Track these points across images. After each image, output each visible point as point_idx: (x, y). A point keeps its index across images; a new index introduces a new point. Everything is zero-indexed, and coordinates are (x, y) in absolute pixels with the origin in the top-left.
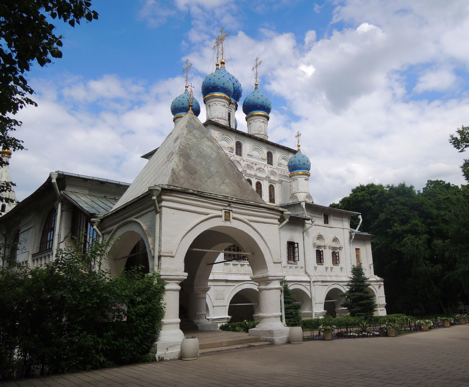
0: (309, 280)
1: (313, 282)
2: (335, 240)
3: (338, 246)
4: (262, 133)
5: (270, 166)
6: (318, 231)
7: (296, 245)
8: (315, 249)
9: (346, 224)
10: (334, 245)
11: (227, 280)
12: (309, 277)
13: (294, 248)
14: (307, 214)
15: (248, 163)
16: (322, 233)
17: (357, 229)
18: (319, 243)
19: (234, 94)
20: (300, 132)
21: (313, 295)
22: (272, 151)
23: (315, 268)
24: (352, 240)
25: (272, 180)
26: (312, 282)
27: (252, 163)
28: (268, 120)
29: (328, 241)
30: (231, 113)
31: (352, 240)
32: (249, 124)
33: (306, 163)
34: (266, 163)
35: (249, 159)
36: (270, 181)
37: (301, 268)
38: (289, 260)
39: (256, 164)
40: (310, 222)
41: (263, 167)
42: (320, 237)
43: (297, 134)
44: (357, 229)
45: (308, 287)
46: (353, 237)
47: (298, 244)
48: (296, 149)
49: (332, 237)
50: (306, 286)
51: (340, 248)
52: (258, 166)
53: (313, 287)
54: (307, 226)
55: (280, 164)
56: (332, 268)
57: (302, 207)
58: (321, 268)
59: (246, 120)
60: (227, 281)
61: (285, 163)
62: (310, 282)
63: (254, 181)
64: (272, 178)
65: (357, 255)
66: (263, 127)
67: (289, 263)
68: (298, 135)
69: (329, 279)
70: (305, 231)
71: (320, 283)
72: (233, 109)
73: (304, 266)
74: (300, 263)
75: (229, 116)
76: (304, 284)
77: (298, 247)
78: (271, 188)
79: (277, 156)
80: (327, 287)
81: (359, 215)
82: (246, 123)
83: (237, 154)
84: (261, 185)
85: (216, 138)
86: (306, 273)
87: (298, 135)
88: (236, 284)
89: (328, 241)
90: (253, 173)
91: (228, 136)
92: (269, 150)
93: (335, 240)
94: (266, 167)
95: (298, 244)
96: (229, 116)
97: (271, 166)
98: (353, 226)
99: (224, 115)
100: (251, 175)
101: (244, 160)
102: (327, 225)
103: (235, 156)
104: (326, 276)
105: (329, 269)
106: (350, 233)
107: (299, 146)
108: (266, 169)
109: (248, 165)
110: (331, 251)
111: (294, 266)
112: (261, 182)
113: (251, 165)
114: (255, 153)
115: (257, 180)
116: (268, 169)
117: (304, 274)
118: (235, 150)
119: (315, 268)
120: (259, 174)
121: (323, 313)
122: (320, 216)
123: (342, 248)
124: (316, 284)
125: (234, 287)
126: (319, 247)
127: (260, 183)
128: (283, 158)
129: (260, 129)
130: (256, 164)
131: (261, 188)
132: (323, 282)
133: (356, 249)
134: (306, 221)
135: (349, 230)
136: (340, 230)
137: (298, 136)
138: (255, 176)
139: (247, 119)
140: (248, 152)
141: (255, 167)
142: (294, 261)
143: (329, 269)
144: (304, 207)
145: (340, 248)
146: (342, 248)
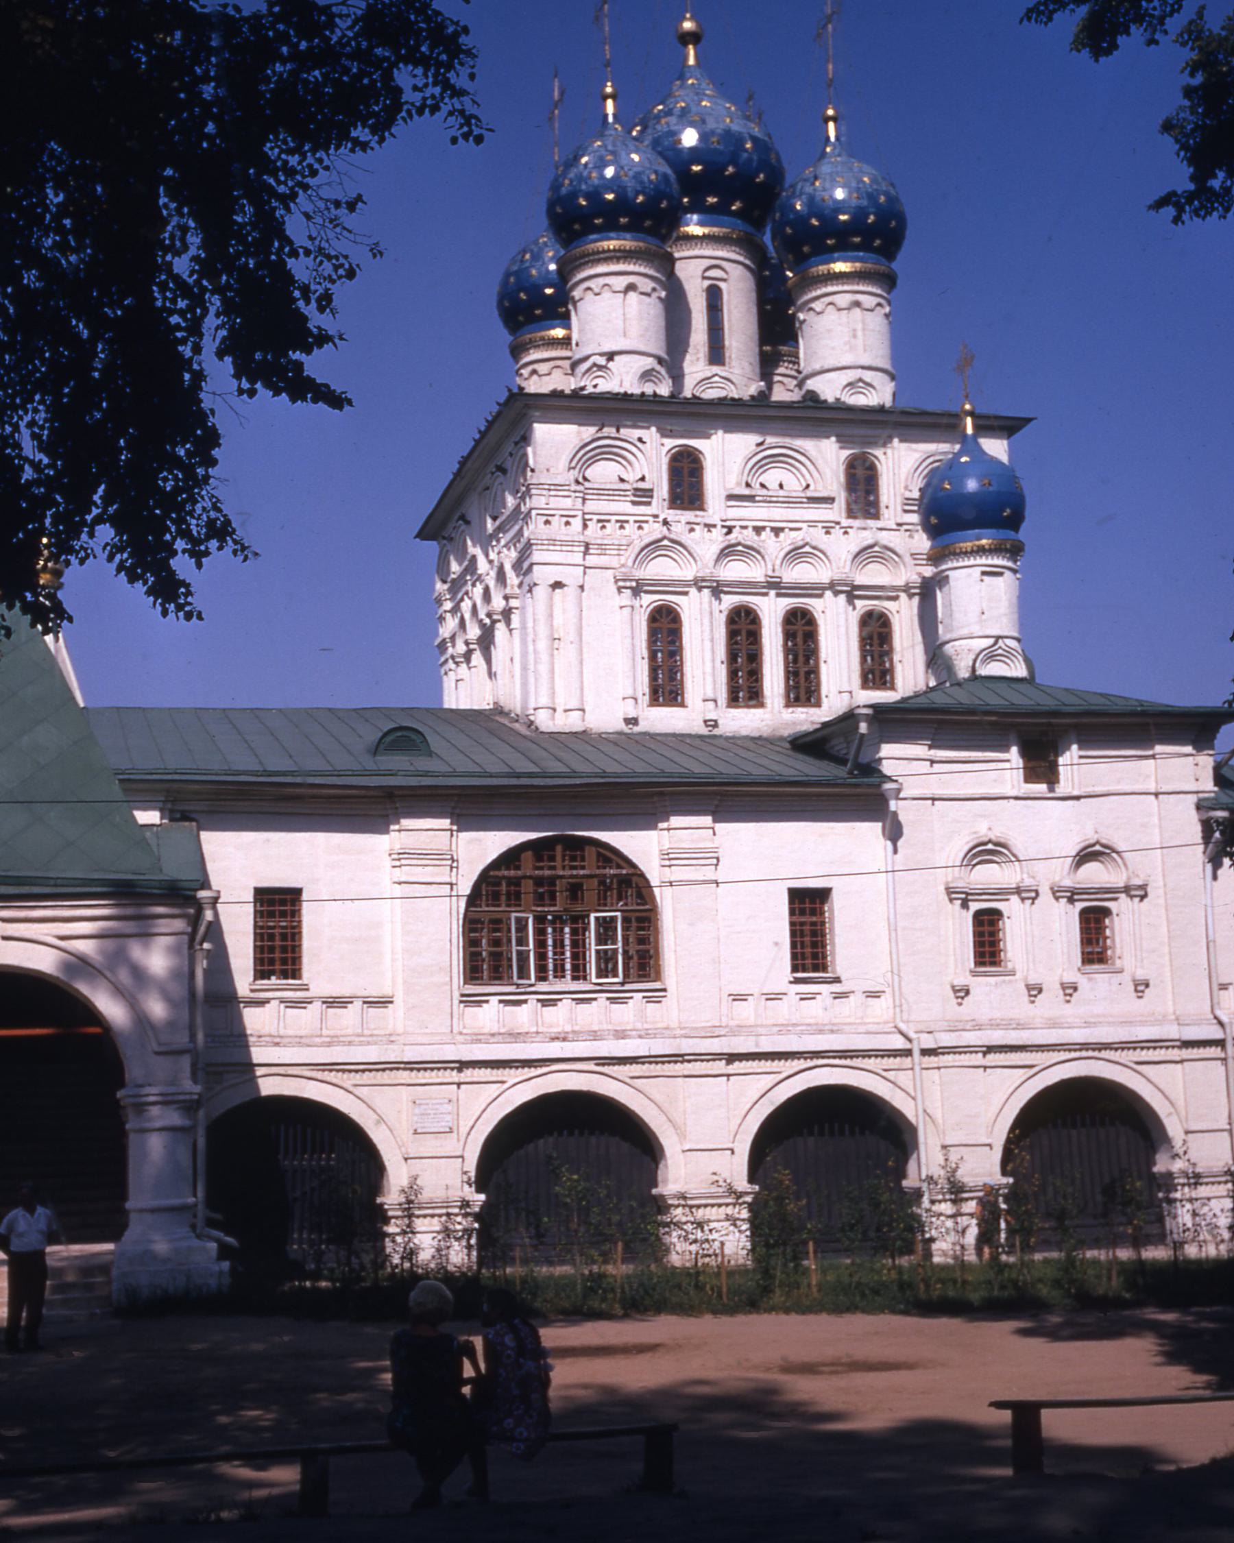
27: (758, 530)
30: (722, 285)
34: (836, 512)
38: (795, 969)
39: (777, 531)
41: (817, 536)
51: (1139, 892)
52: (789, 539)
56: (1070, 989)
62: (908, 1053)
71: (978, 1059)
88: (512, 1075)
94: (837, 532)
105: (1052, 993)
115: (786, 603)
125: (494, 1089)
138: (775, 585)
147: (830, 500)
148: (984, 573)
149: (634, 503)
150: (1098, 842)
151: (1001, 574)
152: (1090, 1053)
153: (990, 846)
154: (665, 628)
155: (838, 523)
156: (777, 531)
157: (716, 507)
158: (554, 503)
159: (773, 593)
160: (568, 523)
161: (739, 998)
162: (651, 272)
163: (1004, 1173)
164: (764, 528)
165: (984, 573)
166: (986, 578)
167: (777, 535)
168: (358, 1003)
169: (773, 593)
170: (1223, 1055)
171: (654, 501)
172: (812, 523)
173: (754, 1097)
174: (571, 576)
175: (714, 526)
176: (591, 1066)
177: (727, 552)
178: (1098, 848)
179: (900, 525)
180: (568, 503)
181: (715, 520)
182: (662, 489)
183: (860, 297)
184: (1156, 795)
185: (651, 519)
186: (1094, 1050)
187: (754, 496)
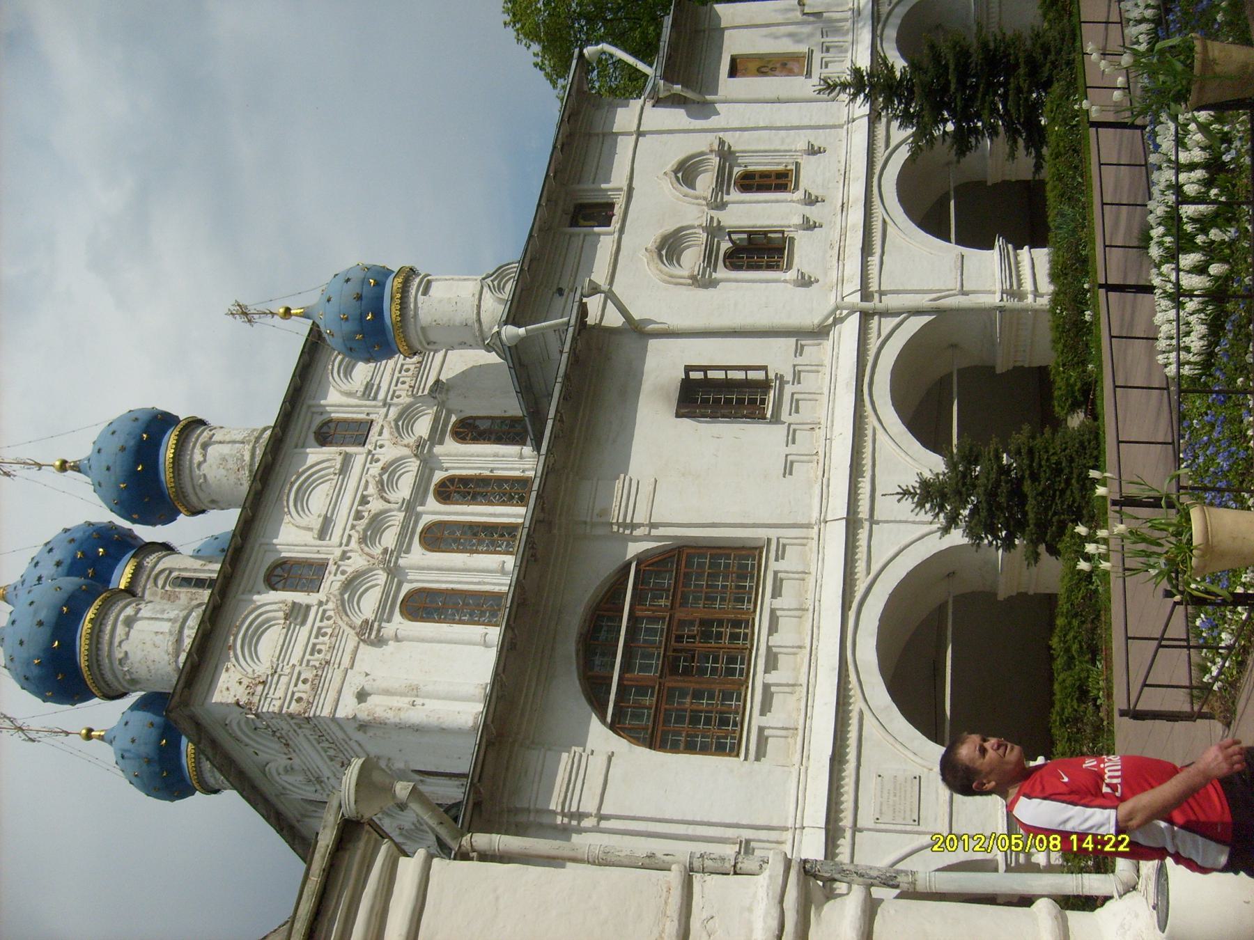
0: (853, 322)
1: (866, 295)
2: (686, 172)
3: (715, 161)
4: (247, 458)
5: (373, 436)
6: (644, 258)
7: (695, 375)
8: (722, 273)
9: (625, 117)
10: (706, 182)
11: (832, 759)
12: (838, 321)
13: (707, 384)
14: (556, 320)
16: (651, 240)
17: (641, 66)
18: (692, 258)
19: (95, 566)
20: (229, 304)
21: (924, 301)
22: (318, 421)
23: (805, 282)
24: (689, 94)
25: (434, 429)
26: (867, 305)
27: (359, 516)
28: (201, 423)
29: (689, 211)
30: (175, 574)
31: (689, 94)
32: (216, 504)
33: (352, 288)
35: (337, 532)
36: (436, 436)
37: (799, 351)
40: (594, 304)
41: (375, 469)
42: (670, 247)
43: (239, 320)
44: (641, 66)
45: (889, 323)
46: (678, 88)
47: (688, 369)
48: (305, 327)
49: (669, 190)
50: (884, 334)
52: (372, 490)
53: (890, 302)
54: (614, 319)
55: (369, 390)
56: (811, 200)
57: (522, 340)
58: (806, 253)
59: (203, 511)
60: (837, 760)
61: (362, 371)
62: (866, 316)
63: (433, 510)
64: (423, 427)
65: (761, 72)
66: (225, 449)
68: (244, 313)
69: (856, 216)
70: (639, 331)
71: (874, 260)
72: (160, 567)
73: (792, 341)
74: (774, 357)
75: (187, 582)
76: (873, 345)
77: (704, 369)
78: (469, 430)
79: (340, 394)
80: (891, 229)
81: (581, 55)
82: (213, 514)
83: (313, 585)
84: (451, 479)
85: (246, 682)
86: (821, 332)
87: (244, 313)
88: (856, 704)
89: (689, 211)
91: (240, 628)
92: (311, 437)
93: (686, 172)
95: (688, 369)
96: (187, 582)
97: (375, 429)
98: (633, 84)
99: (166, 627)
100: (404, 527)
101: (344, 556)
102: (618, 211)
103: (321, 596)
104: (843, 234)
105: (814, 213)
106: (658, 102)
107: (288, 310)
108: (388, 453)
109: (363, 540)
110: (735, 195)
111: (788, 390)
112: (439, 476)
113: (364, 522)
114: (318, 500)
116: (387, 446)
117: (827, 344)
118: (300, 597)
119: (805, 282)
120: (404, 489)
121: (1004, 256)
122: (576, 242)
123: (722, 142)
124: (874, 287)
125: (869, 720)
126: (710, 256)
127: (442, 484)
128: (348, 373)
129: (231, 464)
131: (465, 481)
132: (866, 250)
133: (733, 73)
134: (591, 320)
135: (649, 104)
136: (649, 146)
137: (245, 314)
138: (410, 508)
139: (195, 512)
140: (309, 538)
141: (376, 505)
142: (765, 386)
143: (814, 213)
144: (522, 331)
145: (726, 155)
146: (722, 142)
148: (425, 293)
149: (303, 623)
154: (426, 605)
155: (370, 452)
156: (364, 501)
157: (330, 550)
158: (280, 693)
160: (305, 682)
161: (788, 469)
162: (121, 604)
163: (991, 247)
164: (358, 512)
167: (368, 502)
169: (419, 509)
172: (364, 470)
174: (355, 681)
175: (344, 553)
176: (852, 615)
179: (384, 405)
181: (338, 552)
183: (201, 440)
187: (326, 517)
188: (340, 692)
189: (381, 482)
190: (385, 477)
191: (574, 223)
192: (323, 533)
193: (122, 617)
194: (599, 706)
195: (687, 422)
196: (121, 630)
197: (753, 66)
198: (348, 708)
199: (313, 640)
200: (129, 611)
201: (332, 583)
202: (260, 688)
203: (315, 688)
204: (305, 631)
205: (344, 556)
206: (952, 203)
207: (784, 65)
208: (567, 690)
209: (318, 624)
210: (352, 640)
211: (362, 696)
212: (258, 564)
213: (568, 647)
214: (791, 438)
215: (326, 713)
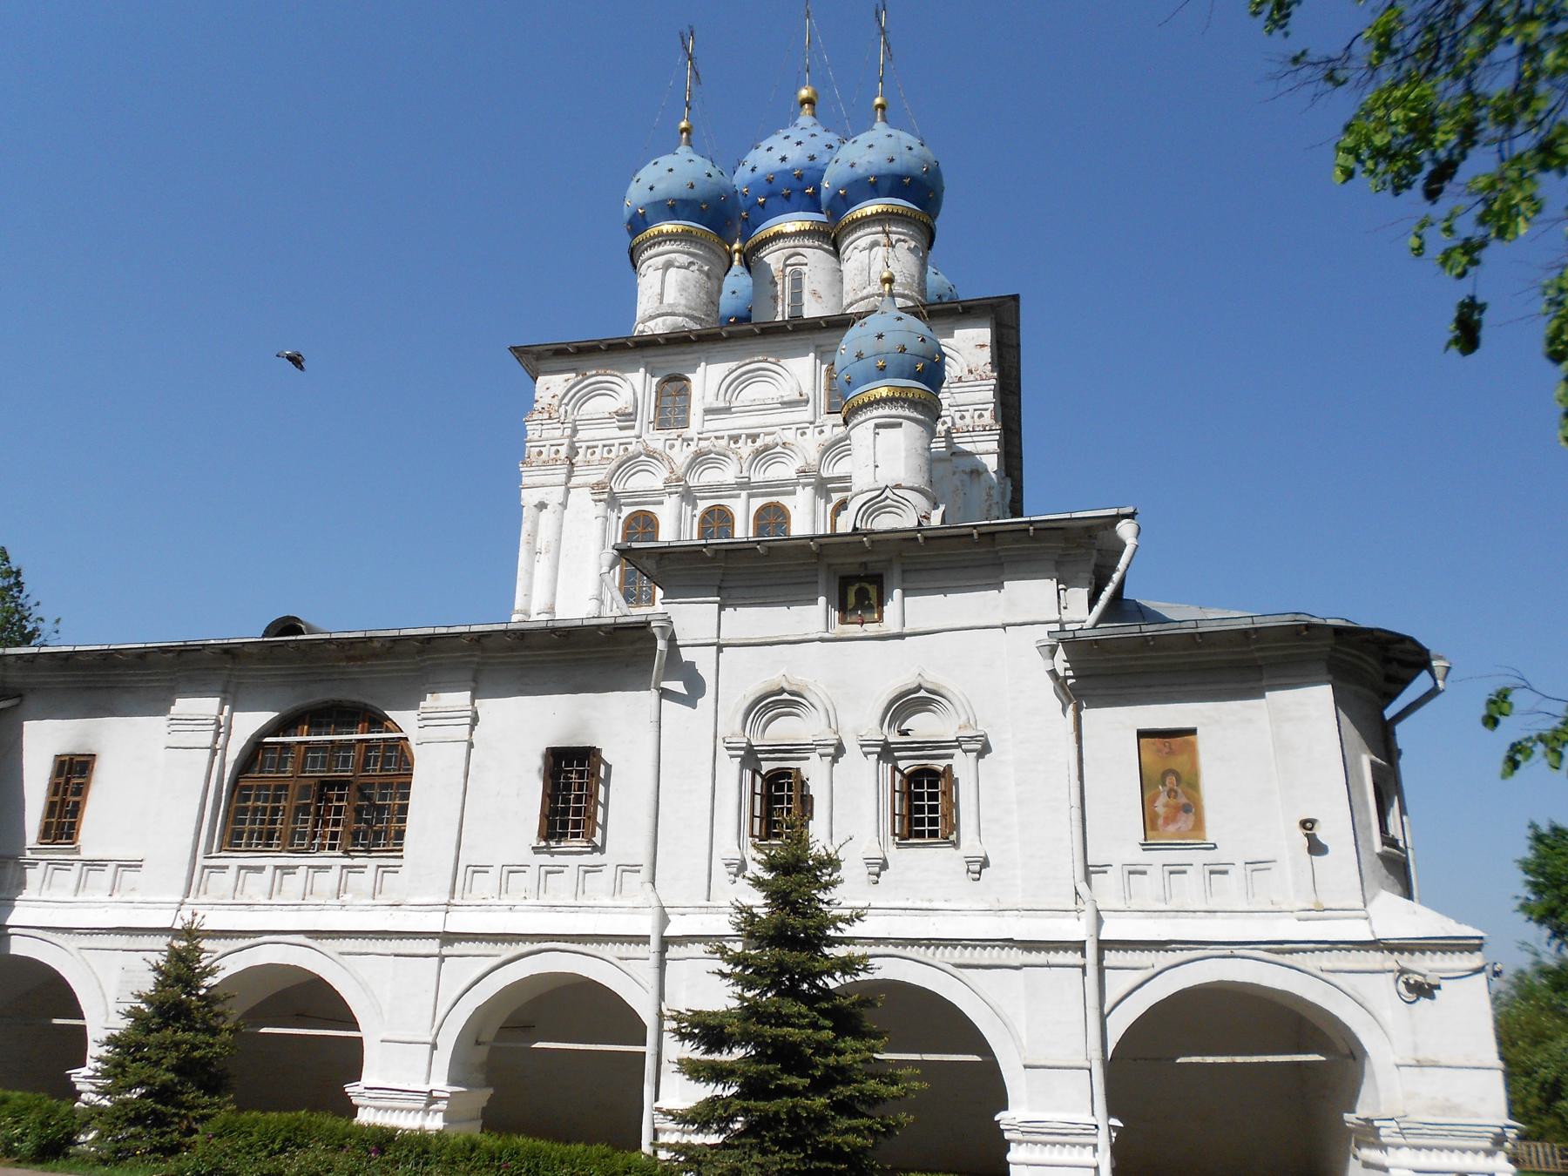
2: (908, 703)
4: (865, 292)
15: (703, 444)
27: (736, 439)
41: (789, 436)
67: (537, 850)
81: (1119, 518)
90: (728, 474)
101: (688, 441)
102: (871, 629)
112: (783, 500)
130: (754, 438)
147: (802, 402)
149: (621, 428)
150: (919, 688)
151: (900, 425)
152: (891, 950)
153: (785, 696)
156: (754, 438)
159: (744, 494)
165: (877, 426)
166: (881, 431)
168: (112, 866)
169: (744, 494)
170: (1080, 961)
171: (637, 424)
172: (785, 427)
173: (475, 982)
176: (301, 939)
177: (700, 459)
178: (922, 693)
180: (558, 433)
182: (648, 410)
184: (1004, 627)
185: (634, 440)
186: (896, 946)
188: (543, 486)
189: (767, 448)
190: (779, 449)
191: (845, 582)
192: (707, 411)
193: (673, 255)
194: (283, 725)
195: (537, 762)
196: (661, 260)
197: (1179, 762)
198: (529, 498)
199: (600, 444)
200: (685, 259)
201: (657, 440)
202: (546, 416)
203: (545, 463)
204: (612, 432)
205: (687, 441)
206: (976, 1058)
207: (1186, 809)
208: (295, 700)
209: (616, 442)
210: (594, 479)
211: (542, 506)
212: (672, 362)
213: (319, 694)
214: (516, 870)
215: (525, 480)
